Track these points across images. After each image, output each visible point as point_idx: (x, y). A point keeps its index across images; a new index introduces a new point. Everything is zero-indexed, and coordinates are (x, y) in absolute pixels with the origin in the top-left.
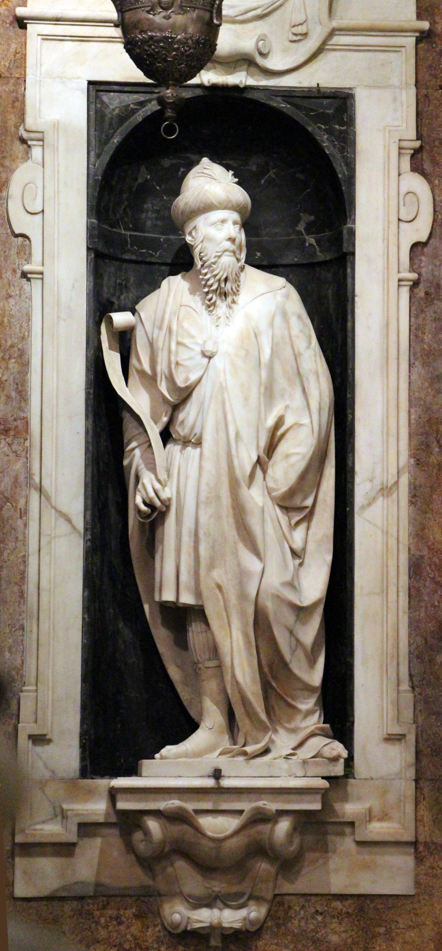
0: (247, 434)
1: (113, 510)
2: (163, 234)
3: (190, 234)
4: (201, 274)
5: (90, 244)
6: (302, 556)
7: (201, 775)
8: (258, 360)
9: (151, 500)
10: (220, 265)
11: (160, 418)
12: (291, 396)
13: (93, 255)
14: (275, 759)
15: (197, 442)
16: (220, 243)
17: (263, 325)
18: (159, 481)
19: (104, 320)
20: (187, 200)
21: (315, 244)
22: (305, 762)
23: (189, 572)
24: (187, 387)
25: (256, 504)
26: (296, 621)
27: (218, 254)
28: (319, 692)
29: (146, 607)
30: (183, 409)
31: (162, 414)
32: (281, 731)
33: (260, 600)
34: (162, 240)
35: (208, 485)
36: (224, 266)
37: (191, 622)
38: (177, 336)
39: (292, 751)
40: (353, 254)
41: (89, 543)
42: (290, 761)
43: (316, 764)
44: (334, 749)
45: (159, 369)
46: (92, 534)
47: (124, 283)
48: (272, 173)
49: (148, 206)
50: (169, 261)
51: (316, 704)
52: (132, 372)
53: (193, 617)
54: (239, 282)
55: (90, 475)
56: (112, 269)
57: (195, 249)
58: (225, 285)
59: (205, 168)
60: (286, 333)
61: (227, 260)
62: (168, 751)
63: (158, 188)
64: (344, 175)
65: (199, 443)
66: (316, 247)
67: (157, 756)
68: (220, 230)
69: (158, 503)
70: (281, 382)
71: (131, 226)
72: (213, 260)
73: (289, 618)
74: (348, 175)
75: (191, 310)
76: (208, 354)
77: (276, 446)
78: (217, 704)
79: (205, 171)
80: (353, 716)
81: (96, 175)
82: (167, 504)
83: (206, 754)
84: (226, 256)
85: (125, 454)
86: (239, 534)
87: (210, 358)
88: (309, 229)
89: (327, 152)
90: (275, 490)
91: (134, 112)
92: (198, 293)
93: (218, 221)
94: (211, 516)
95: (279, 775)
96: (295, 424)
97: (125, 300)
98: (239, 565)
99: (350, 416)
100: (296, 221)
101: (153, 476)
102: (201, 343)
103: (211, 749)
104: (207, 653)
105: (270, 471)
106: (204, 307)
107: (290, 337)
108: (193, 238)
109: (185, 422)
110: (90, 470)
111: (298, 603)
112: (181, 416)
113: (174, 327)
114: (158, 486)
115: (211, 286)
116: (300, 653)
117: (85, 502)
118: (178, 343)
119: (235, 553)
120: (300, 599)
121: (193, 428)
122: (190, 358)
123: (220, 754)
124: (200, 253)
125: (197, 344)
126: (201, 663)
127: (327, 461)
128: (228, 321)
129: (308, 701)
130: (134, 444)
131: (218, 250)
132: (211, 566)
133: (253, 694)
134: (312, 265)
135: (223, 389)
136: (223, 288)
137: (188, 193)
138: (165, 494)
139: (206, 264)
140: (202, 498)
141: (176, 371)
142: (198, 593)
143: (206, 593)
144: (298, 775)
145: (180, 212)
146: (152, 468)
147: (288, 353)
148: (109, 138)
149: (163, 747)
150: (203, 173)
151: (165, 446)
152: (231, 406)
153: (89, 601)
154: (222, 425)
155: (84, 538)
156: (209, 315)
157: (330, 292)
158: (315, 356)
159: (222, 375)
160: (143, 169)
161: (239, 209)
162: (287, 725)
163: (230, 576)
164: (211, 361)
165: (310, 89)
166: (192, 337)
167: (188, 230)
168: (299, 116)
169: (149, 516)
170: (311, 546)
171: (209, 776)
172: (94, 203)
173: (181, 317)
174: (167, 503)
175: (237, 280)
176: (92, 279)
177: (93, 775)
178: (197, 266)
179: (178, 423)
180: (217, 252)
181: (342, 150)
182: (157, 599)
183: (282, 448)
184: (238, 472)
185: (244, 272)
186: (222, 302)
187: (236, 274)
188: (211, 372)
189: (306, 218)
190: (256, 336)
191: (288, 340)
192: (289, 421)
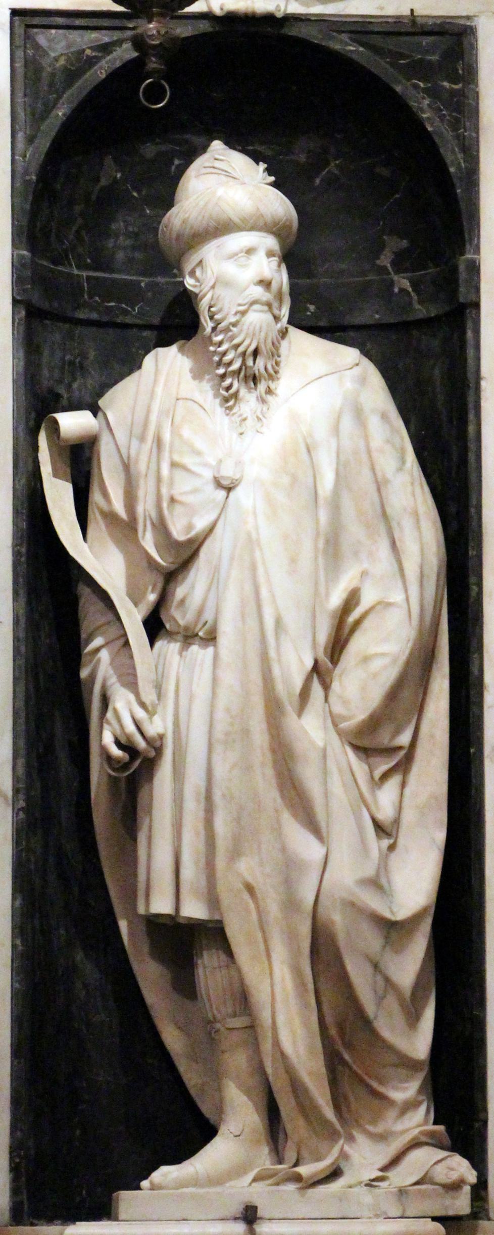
0: (295, 622)
1: (62, 756)
2: (144, 274)
3: (192, 273)
4: (211, 343)
5: (19, 294)
6: (394, 833)
7: (221, 1216)
8: (313, 492)
9: (129, 737)
10: (245, 327)
11: (144, 595)
12: (371, 554)
13: (23, 313)
14: (350, 1187)
15: (208, 637)
16: (245, 290)
17: (322, 432)
18: (143, 705)
19: (43, 425)
20: (187, 215)
21: (410, 290)
22: (402, 1192)
23: (196, 863)
24: (190, 541)
25: (312, 743)
26: (384, 947)
27: (242, 308)
28: (426, 1069)
29: (123, 925)
30: (184, 578)
31: (147, 589)
32: (360, 1138)
33: (321, 910)
34: (143, 284)
35: (228, 710)
36: (251, 329)
37: (201, 949)
38: (171, 452)
39: (380, 1174)
40: (477, 305)
41: (22, 815)
42: (377, 1190)
43: (423, 1195)
44: (452, 1169)
45: (140, 509)
46: (28, 799)
47: (77, 360)
48: (333, 167)
49: (118, 225)
50: (156, 321)
51: (420, 1091)
52: (94, 516)
53: (204, 942)
54: (279, 356)
55: (21, 696)
56: (57, 337)
57: (201, 300)
58: (254, 363)
59: (216, 159)
60: (362, 444)
61: (258, 318)
62: (165, 1175)
63: (135, 194)
64: (459, 168)
65: (211, 638)
66: (413, 294)
67: (145, 1184)
68: (244, 266)
69: (141, 744)
70: (354, 530)
71: (89, 261)
72: (233, 319)
73: (373, 941)
74: (466, 168)
75: (196, 406)
76: (225, 483)
77: (347, 641)
78: (248, 1092)
79: (217, 164)
80: (485, 1110)
81: (26, 172)
82: (157, 745)
83: (231, 1180)
84: (255, 311)
85: (83, 660)
86: (283, 797)
87: (229, 489)
88: (399, 264)
89: (430, 129)
90: (345, 719)
91: (91, 62)
92: (207, 377)
93: (241, 252)
94: (234, 766)
95: (358, 1215)
96: (379, 603)
97: (80, 391)
98: (284, 849)
99: (475, 588)
101: (132, 697)
102: (214, 463)
103: (238, 1171)
104: (230, 1003)
105: (335, 686)
106: (218, 401)
107: (369, 451)
108: (197, 280)
109: (187, 602)
110: (22, 688)
111: (387, 915)
112: (180, 592)
113: (167, 436)
114: (140, 714)
115: (230, 364)
116: (391, 1001)
117: (15, 744)
118: (174, 465)
119: (277, 830)
120: (390, 908)
121: (200, 612)
122: (195, 491)
123: (255, 1180)
124: (210, 307)
125: (206, 465)
126: (219, 1022)
127: (434, 666)
128: (259, 425)
129: (406, 1085)
130: (98, 642)
131: (240, 302)
132: (235, 853)
133: (310, 1074)
134: (405, 326)
135: (252, 543)
136: (251, 368)
137: (187, 203)
138: (154, 728)
139: (220, 326)
140: (219, 734)
141: (171, 512)
142: (213, 900)
143: (226, 899)
144: (390, 1216)
145: (174, 236)
146: (130, 680)
147: (365, 479)
148: (48, 109)
149: (155, 1168)
150: (214, 167)
151: (152, 644)
152: (266, 572)
153: (22, 915)
154: (252, 604)
155: (13, 805)
156: (227, 415)
157: (437, 372)
158: (412, 484)
159: (250, 519)
160: (109, 161)
161: (276, 229)
162: (371, 1128)
163: (268, 870)
164: (231, 494)
165: (398, 20)
166: (198, 453)
167: (188, 268)
168: (380, 67)
169: (125, 766)
170: (408, 816)
171: (236, 1219)
172: (25, 222)
173: (178, 419)
174: (158, 744)
175: (275, 353)
176: (21, 354)
177: (33, 1218)
178: (204, 330)
179: (175, 603)
180: (240, 305)
181: (455, 125)
182: (141, 910)
183: (357, 645)
184: (280, 687)
185: (287, 339)
186: (250, 392)
187: (273, 344)
188: (231, 513)
189: (395, 244)
190: (309, 451)
191: (364, 457)
192: (368, 599)
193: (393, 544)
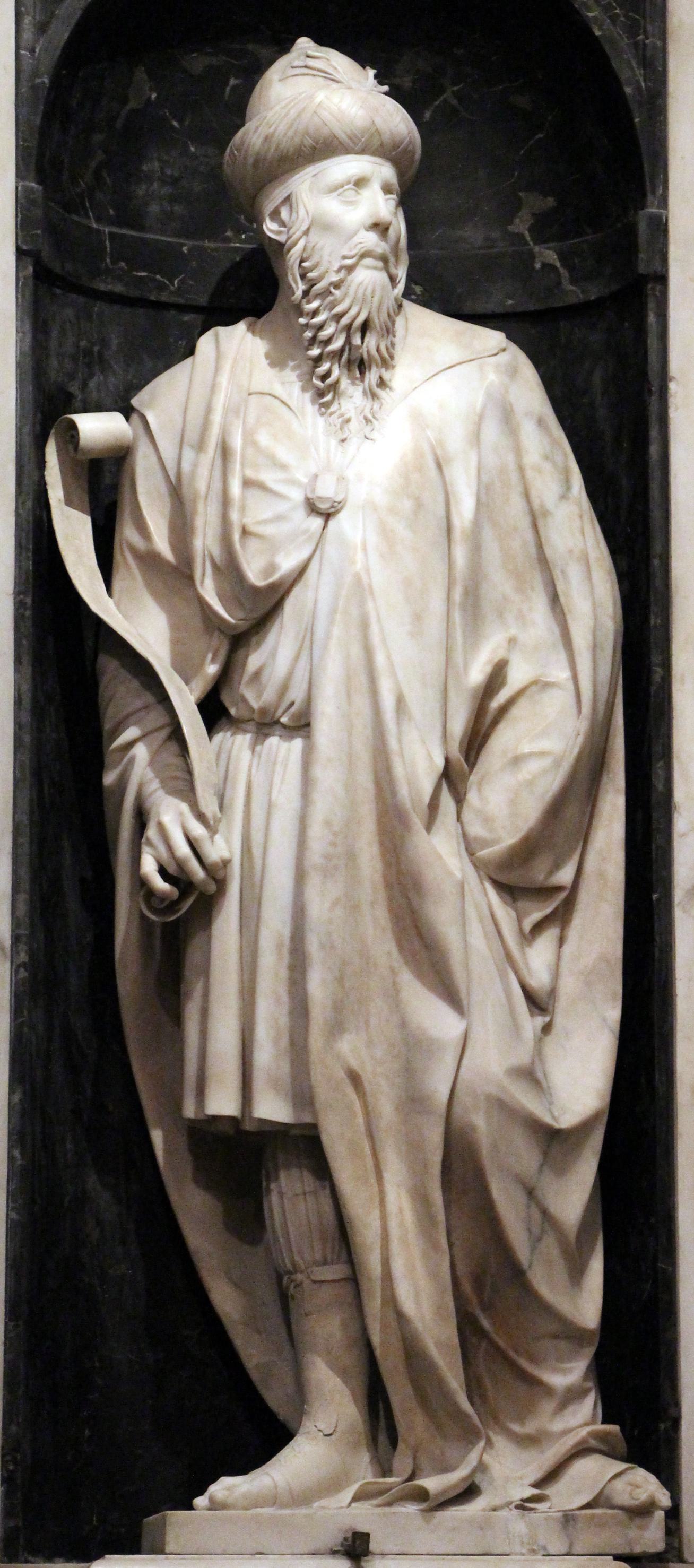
2: (186, 233)
3: (275, 215)
4: (301, 314)
5: (25, 242)
6: (550, 1008)
7: (312, 1549)
8: (444, 524)
9: (180, 864)
10: (352, 292)
11: (202, 664)
12: (521, 617)
13: (31, 269)
14: (494, 1510)
15: (298, 724)
16: (351, 237)
18: (201, 817)
19: (53, 431)
20: (272, 130)
21: (558, 264)
22: (568, 1519)
23: (276, 1041)
24: (272, 587)
25: (450, 874)
26: (542, 1165)
27: (348, 262)
29: (157, 1137)
30: (258, 645)
31: (205, 657)
32: (500, 1442)
33: (457, 1110)
34: (185, 249)
35: (328, 824)
36: (361, 292)
37: (277, 1171)
38: (243, 465)
39: (536, 1491)
40: (662, 279)
41: (23, 974)
42: (532, 1515)
43: (601, 1524)
44: (638, 1487)
45: (198, 544)
46: (31, 953)
47: (96, 349)
48: (449, 96)
49: (151, 166)
50: (203, 300)
51: (586, 1377)
53: (281, 1157)
54: (394, 337)
55: (25, 805)
56: (69, 312)
57: (289, 250)
58: (362, 343)
59: (308, 56)
60: (510, 458)
62: (230, 1488)
63: (175, 123)
64: (638, 88)
66: (562, 270)
67: (200, 1501)
68: (351, 203)
69: (199, 873)
71: (111, 212)
72: (335, 278)
74: (647, 87)
75: (276, 403)
76: (323, 506)
77: (486, 737)
78: (343, 1373)
79: (311, 62)
80: (677, 1404)
81: (35, 73)
83: (320, 1498)
84: (368, 267)
85: (108, 760)
86: (401, 949)
87: (328, 516)
89: (598, 33)
90: (486, 844)
92: (291, 364)
93: (349, 183)
94: (336, 903)
95: (508, 1550)
96: (535, 682)
97: (99, 391)
98: (403, 1024)
99: (658, 672)
100: (512, 208)
101: (185, 807)
102: (305, 480)
104: (318, 1246)
105: (472, 797)
106: (308, 396)
107: (521, 469)
108: (283, 224)
109: (265, 677)
110: (26, 794)
111: (548, 1120)
112: (254, 661)
113: (237, 442)
114: (198, 830)
115: (328, 342)
116: (550, 1246)
117: (15, 872)
118: (247, 483)
120: (550, 1111)
121: (284, 688)
122: (279, 518)
123: (356, 1498)
124: (302, 261)
125: (293, 482)
126: (302, 1272)
127: (605, 778)
128: (369, 428)
129: (569, 1365)
130: (131, 733)
131: (345, 252)
132: (336, 1028)
133: (438, 1345)
136: (359, 347)
137: (270, 114)
138: (216, 850)
139: (315, 287)
141: (243, 545)
143: (322, 1093)
144: (552, 1552)
145: (251, 161)
147: (516, 509)
149: (214, 1480)
150: (306, 67)
151: (210, 738)
152: (382, 630)
153: (23, 1116)
154: (363, 679)
155: (12, 957)
156: (322, 414)
157: (597, 378)
158: (581, 517)
159: (359, 556)
160: (141, 74)
162: (516, 1427)
163: (379, 1053)
164: (331, 523)
166: (283, 467)
167: (269, 207)
169: (173, 906)
170: (569, 986)
171: (334, 1553)
172: (34, 143)
173: (251, 420)
175: (389, 331)
176: (28, 327)
177: (29, 1553)
178: (294, 294)
179: (246, 678)
180: (344, 257)
181: (633, 29)
182: (190, 1111)
184: (404, 792)
185: (402, 313)
186: (353, 384)
187: (389, 315)
188: (331, 549)
190: (439, 466)
191: (514, 477)
192: (517, 677)
193: (555, 599)
